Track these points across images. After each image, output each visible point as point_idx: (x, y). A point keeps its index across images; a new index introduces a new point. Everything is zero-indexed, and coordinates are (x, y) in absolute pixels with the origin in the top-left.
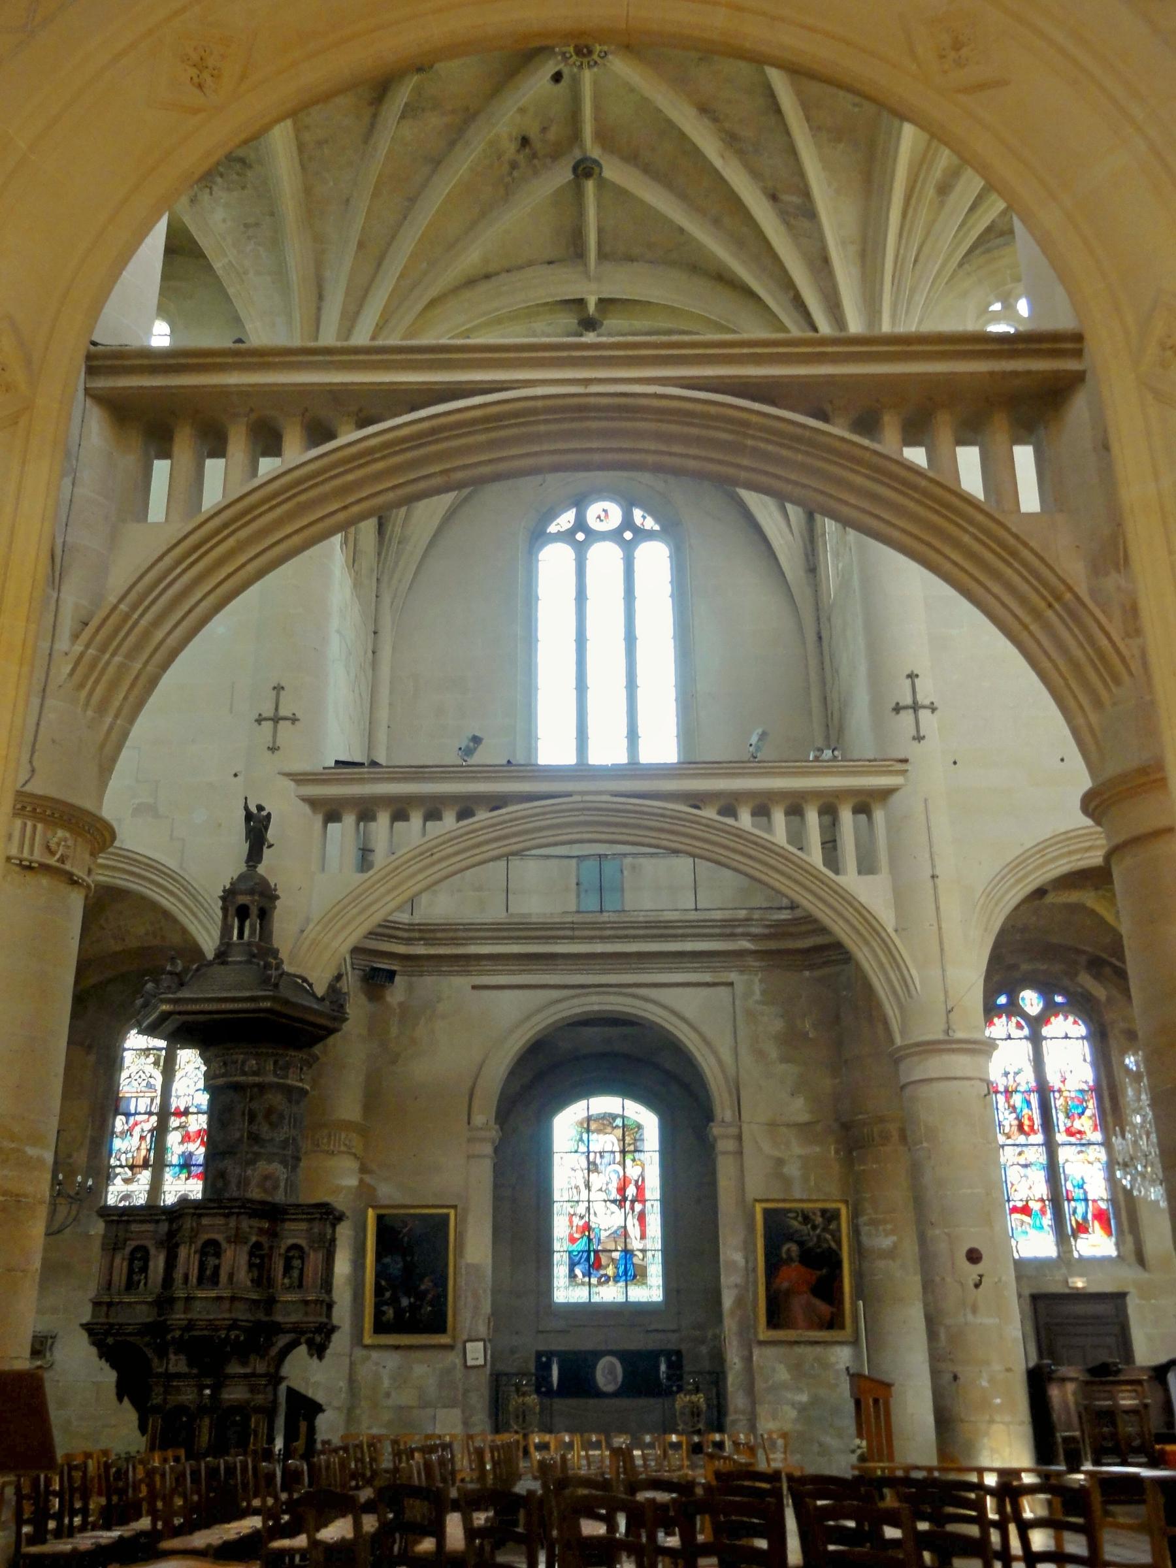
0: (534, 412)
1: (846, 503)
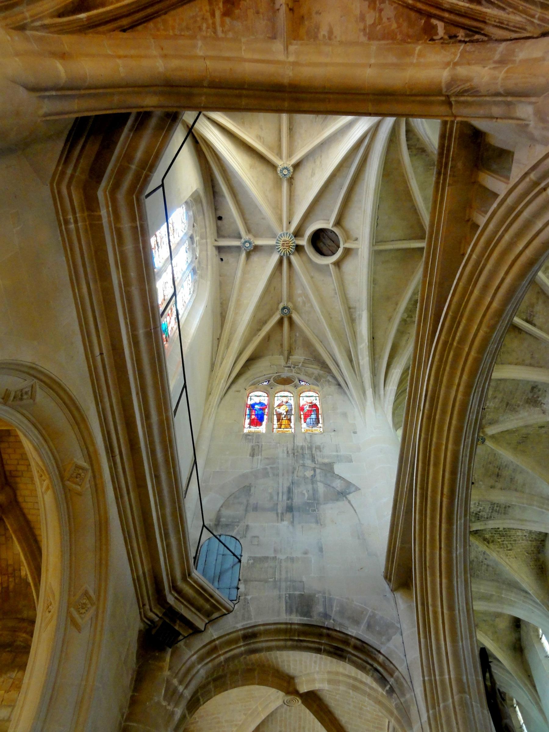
0: (426, 439)
1: (491, 303)
